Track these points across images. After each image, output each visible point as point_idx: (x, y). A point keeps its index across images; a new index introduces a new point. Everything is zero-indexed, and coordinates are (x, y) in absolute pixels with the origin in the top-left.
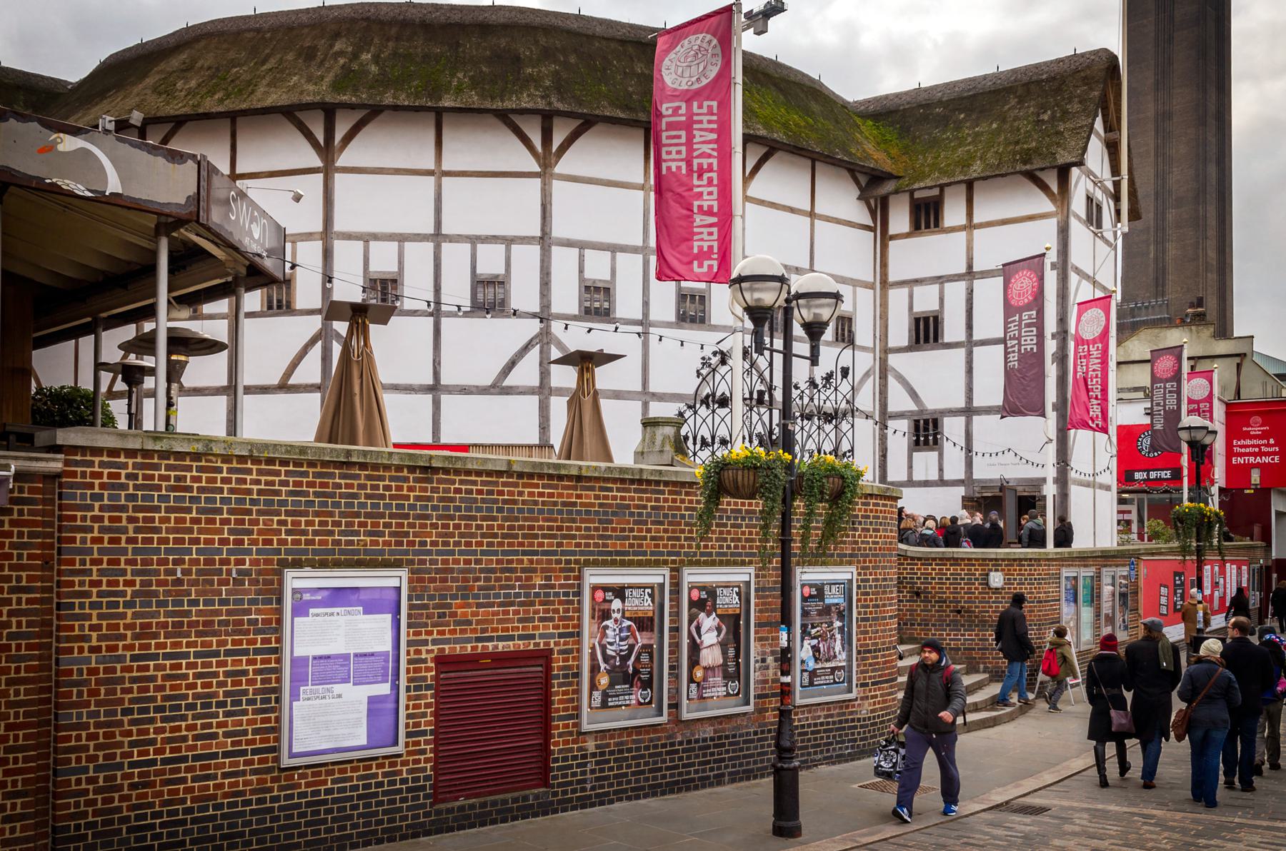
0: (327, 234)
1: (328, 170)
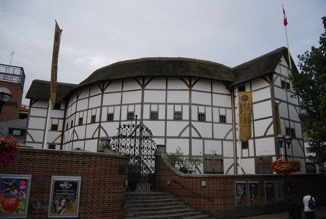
0: (101, 107)
1: (102, 94)
